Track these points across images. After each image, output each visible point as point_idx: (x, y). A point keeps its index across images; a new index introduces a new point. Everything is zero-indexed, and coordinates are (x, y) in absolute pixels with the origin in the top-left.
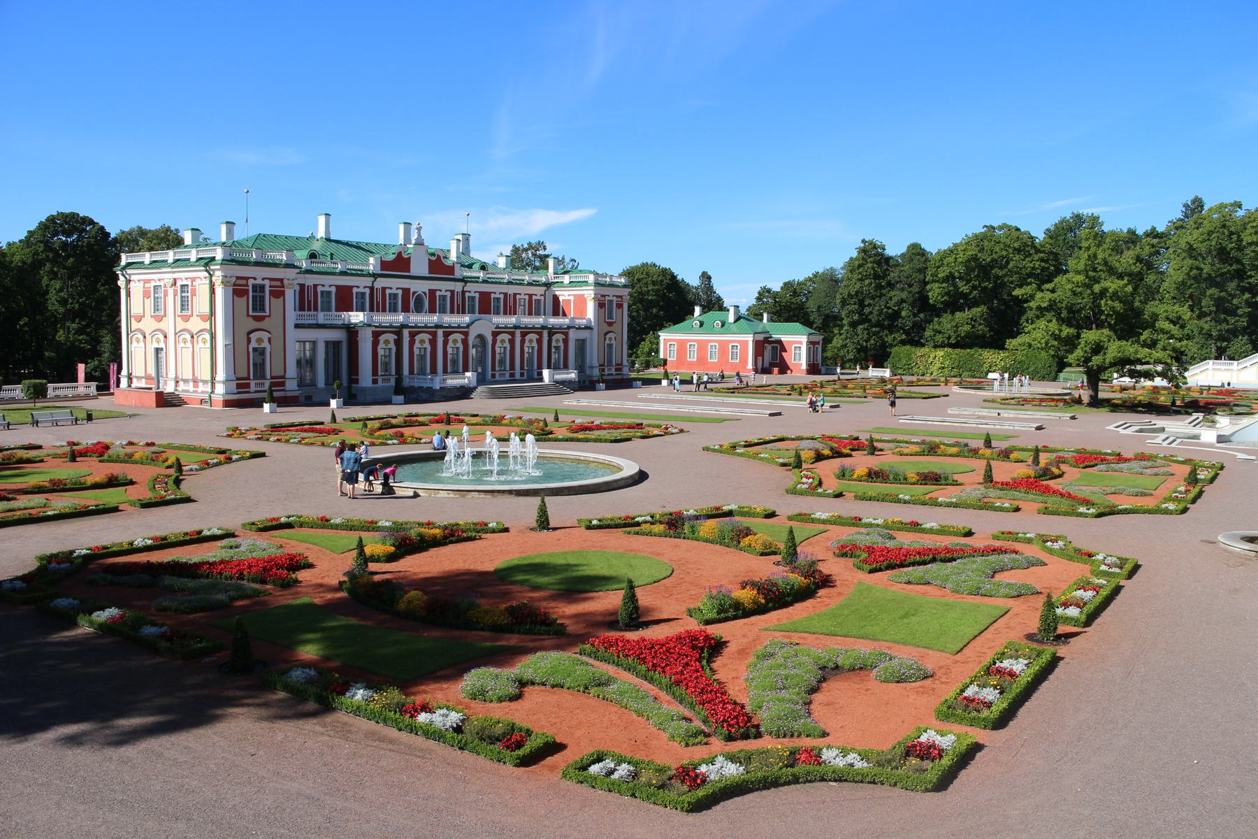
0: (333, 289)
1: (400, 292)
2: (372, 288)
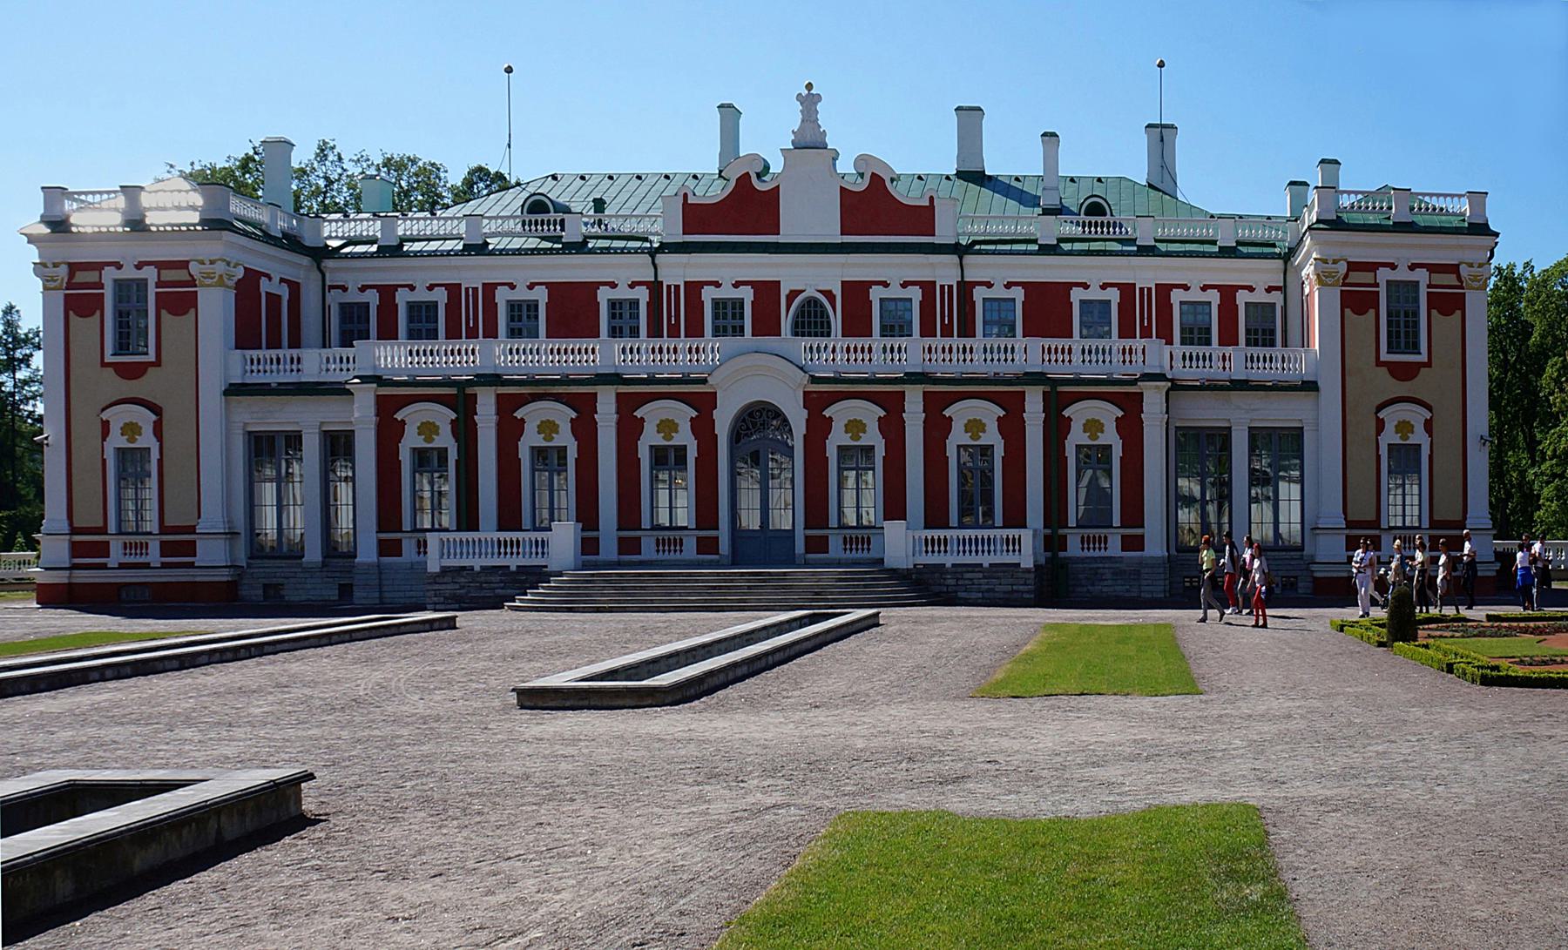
0: (541, 295)
1: (747, 294)
2: (655, 287)
